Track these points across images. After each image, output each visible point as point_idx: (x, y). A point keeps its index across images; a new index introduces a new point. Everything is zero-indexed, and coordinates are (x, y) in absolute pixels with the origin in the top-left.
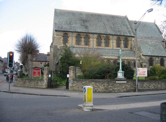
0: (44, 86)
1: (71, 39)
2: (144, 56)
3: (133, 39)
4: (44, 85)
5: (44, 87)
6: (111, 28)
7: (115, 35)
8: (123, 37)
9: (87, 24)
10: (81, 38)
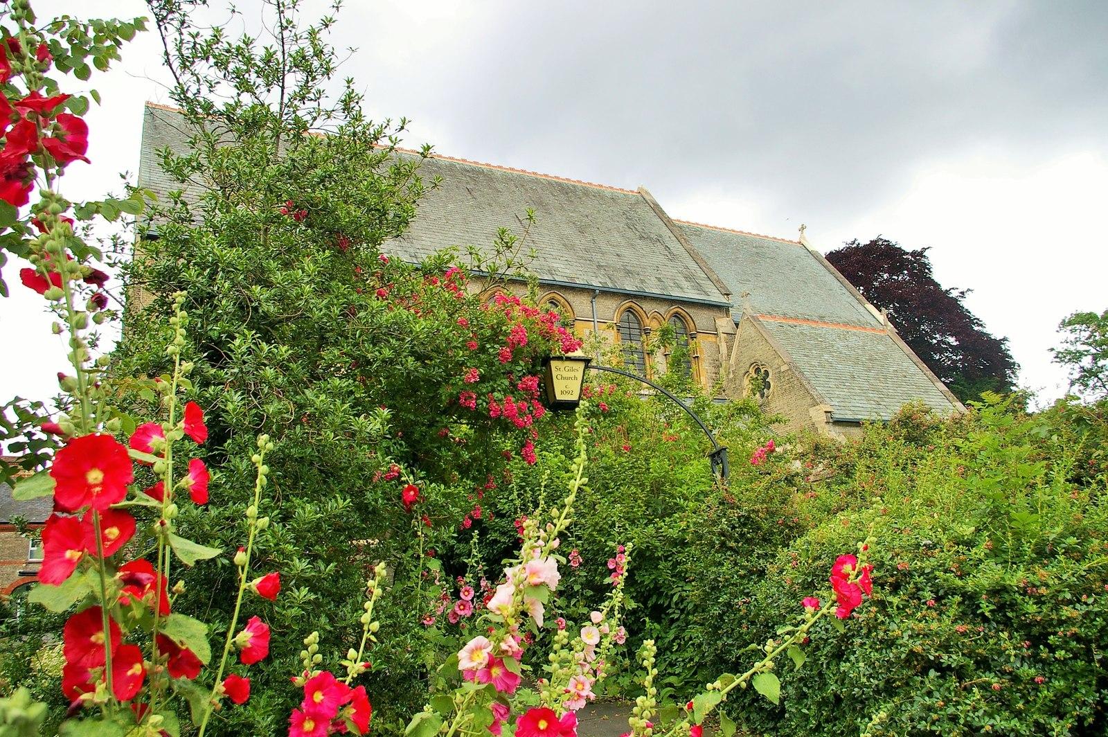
2: (838, 423)
3: (724, 324)
6: (569, 247)
7: (606, 293)
8: (662, 309)
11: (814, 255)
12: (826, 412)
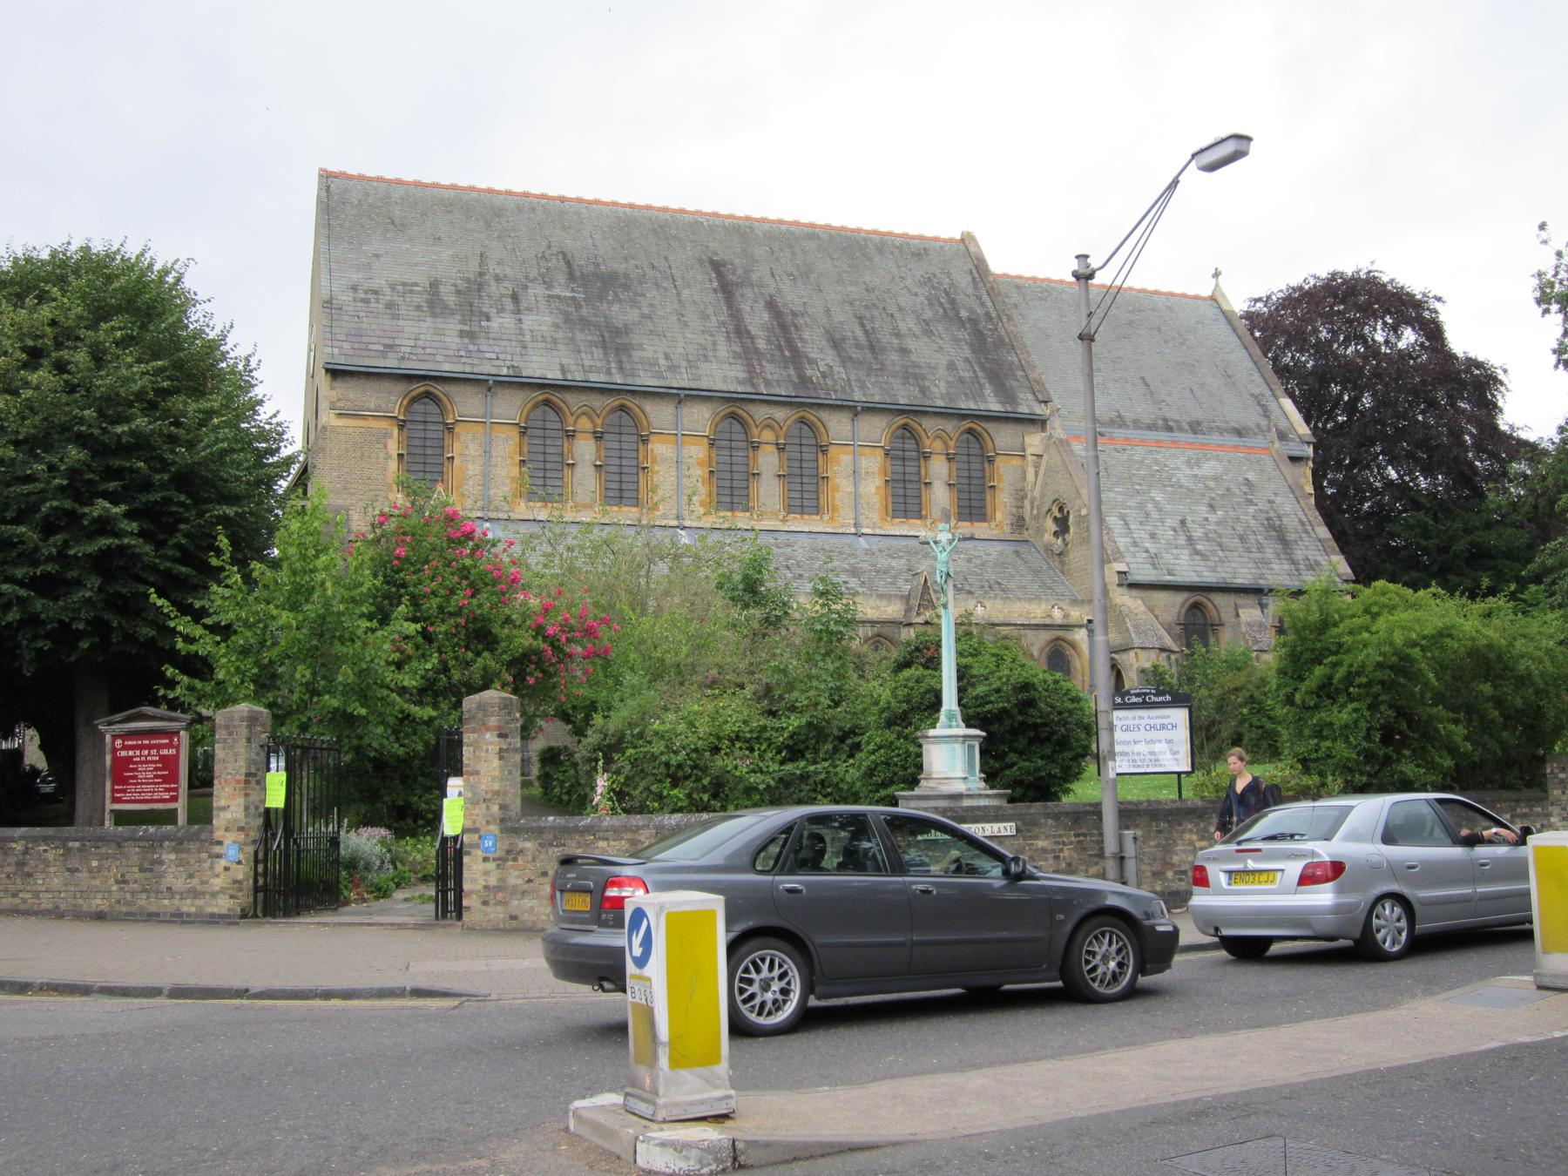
0: (214, 895)
1: (474, 449)
2: (1134, 586)
3: (1034, 441)
4: (223, 891)
5: (223, 905)
7: (871, 409)
8: (950, 426)
9: (621, 314)
10: (571, 435)
11: (1227, 316)
12: (1119, 573)
